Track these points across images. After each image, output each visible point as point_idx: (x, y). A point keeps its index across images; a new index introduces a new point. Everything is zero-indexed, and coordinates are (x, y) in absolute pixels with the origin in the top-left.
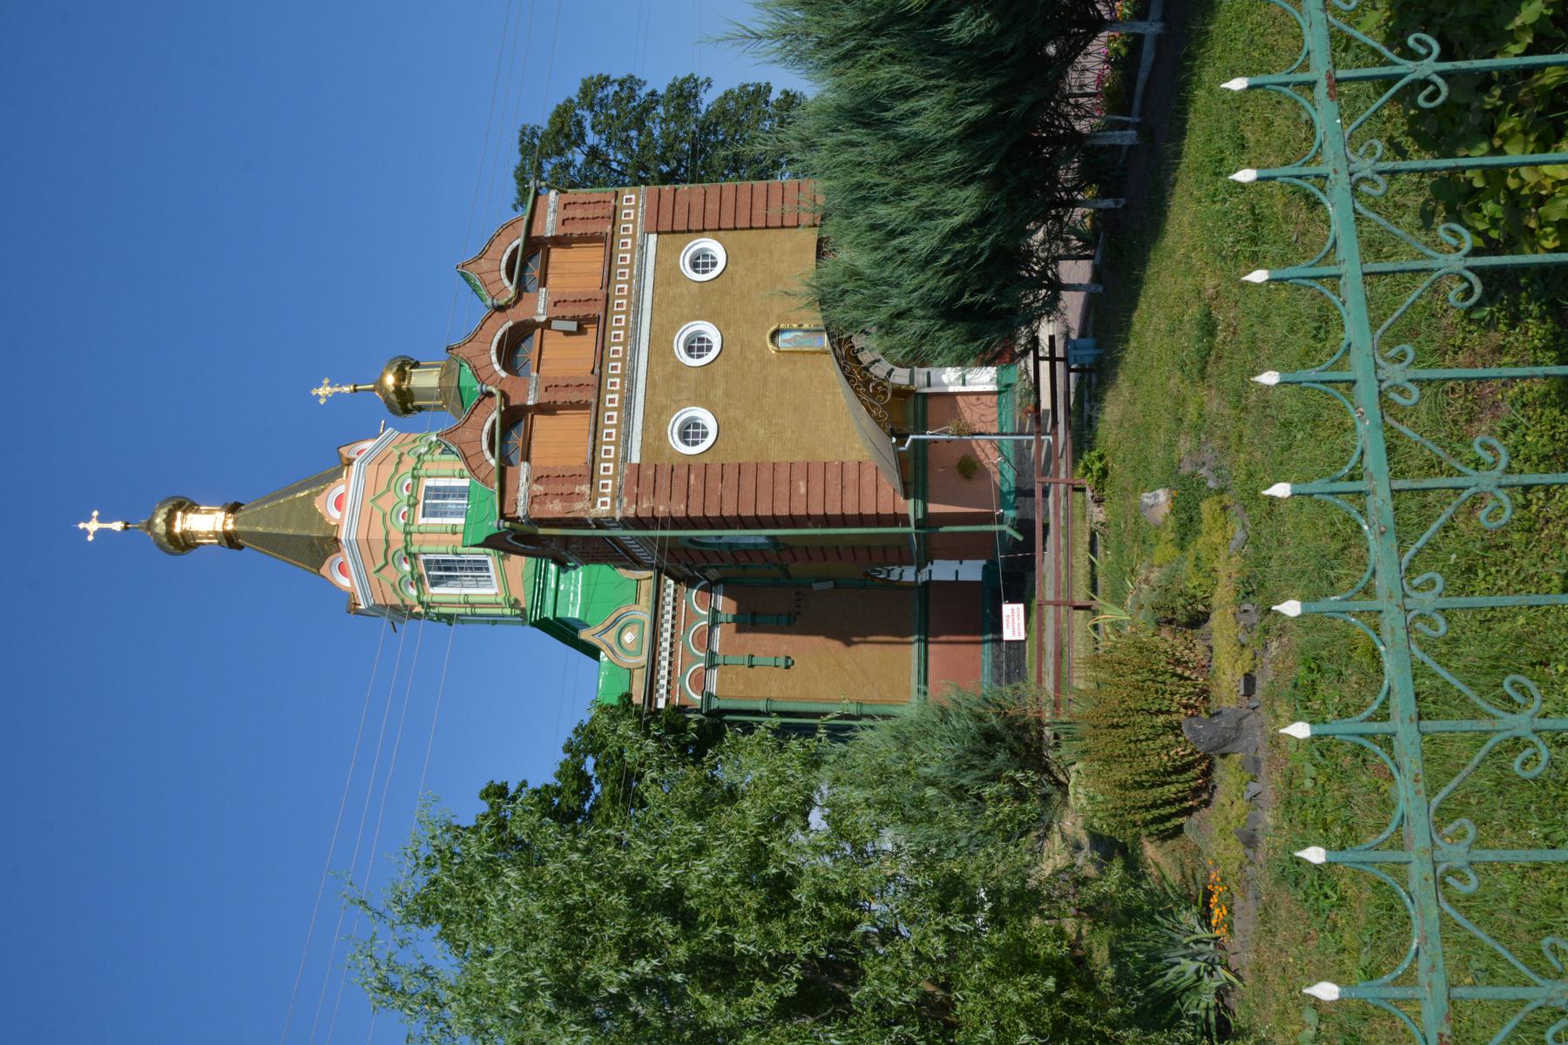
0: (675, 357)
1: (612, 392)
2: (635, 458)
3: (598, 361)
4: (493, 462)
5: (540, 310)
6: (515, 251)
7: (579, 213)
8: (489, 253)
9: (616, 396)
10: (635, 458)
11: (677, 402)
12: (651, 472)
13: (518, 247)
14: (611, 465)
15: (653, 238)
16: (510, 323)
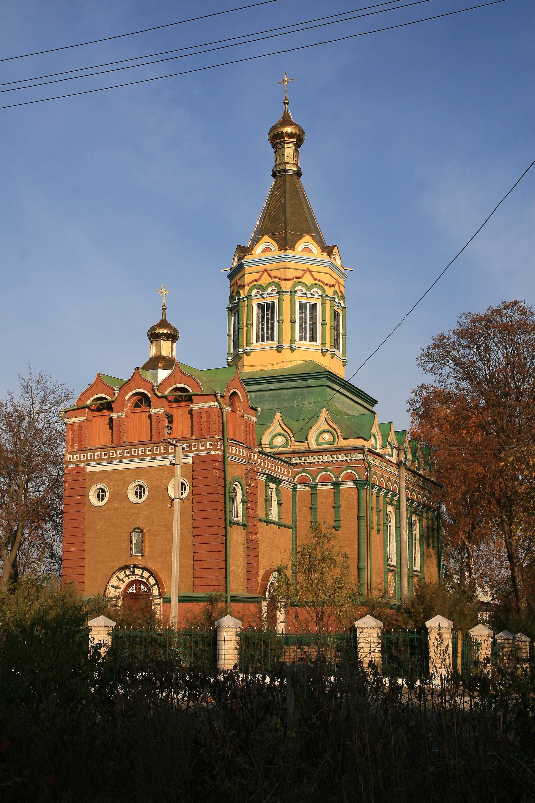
1: (116, 454)
2: (88, 469)
4: (89, 402)
5: (153, 411)
6: (185, 390)
7: (204, 419)
8: (184, 377)
10: (88, 469)
11: (113, 486)
12: (81, 478)
15: (190, 461)
16: (150, 395)
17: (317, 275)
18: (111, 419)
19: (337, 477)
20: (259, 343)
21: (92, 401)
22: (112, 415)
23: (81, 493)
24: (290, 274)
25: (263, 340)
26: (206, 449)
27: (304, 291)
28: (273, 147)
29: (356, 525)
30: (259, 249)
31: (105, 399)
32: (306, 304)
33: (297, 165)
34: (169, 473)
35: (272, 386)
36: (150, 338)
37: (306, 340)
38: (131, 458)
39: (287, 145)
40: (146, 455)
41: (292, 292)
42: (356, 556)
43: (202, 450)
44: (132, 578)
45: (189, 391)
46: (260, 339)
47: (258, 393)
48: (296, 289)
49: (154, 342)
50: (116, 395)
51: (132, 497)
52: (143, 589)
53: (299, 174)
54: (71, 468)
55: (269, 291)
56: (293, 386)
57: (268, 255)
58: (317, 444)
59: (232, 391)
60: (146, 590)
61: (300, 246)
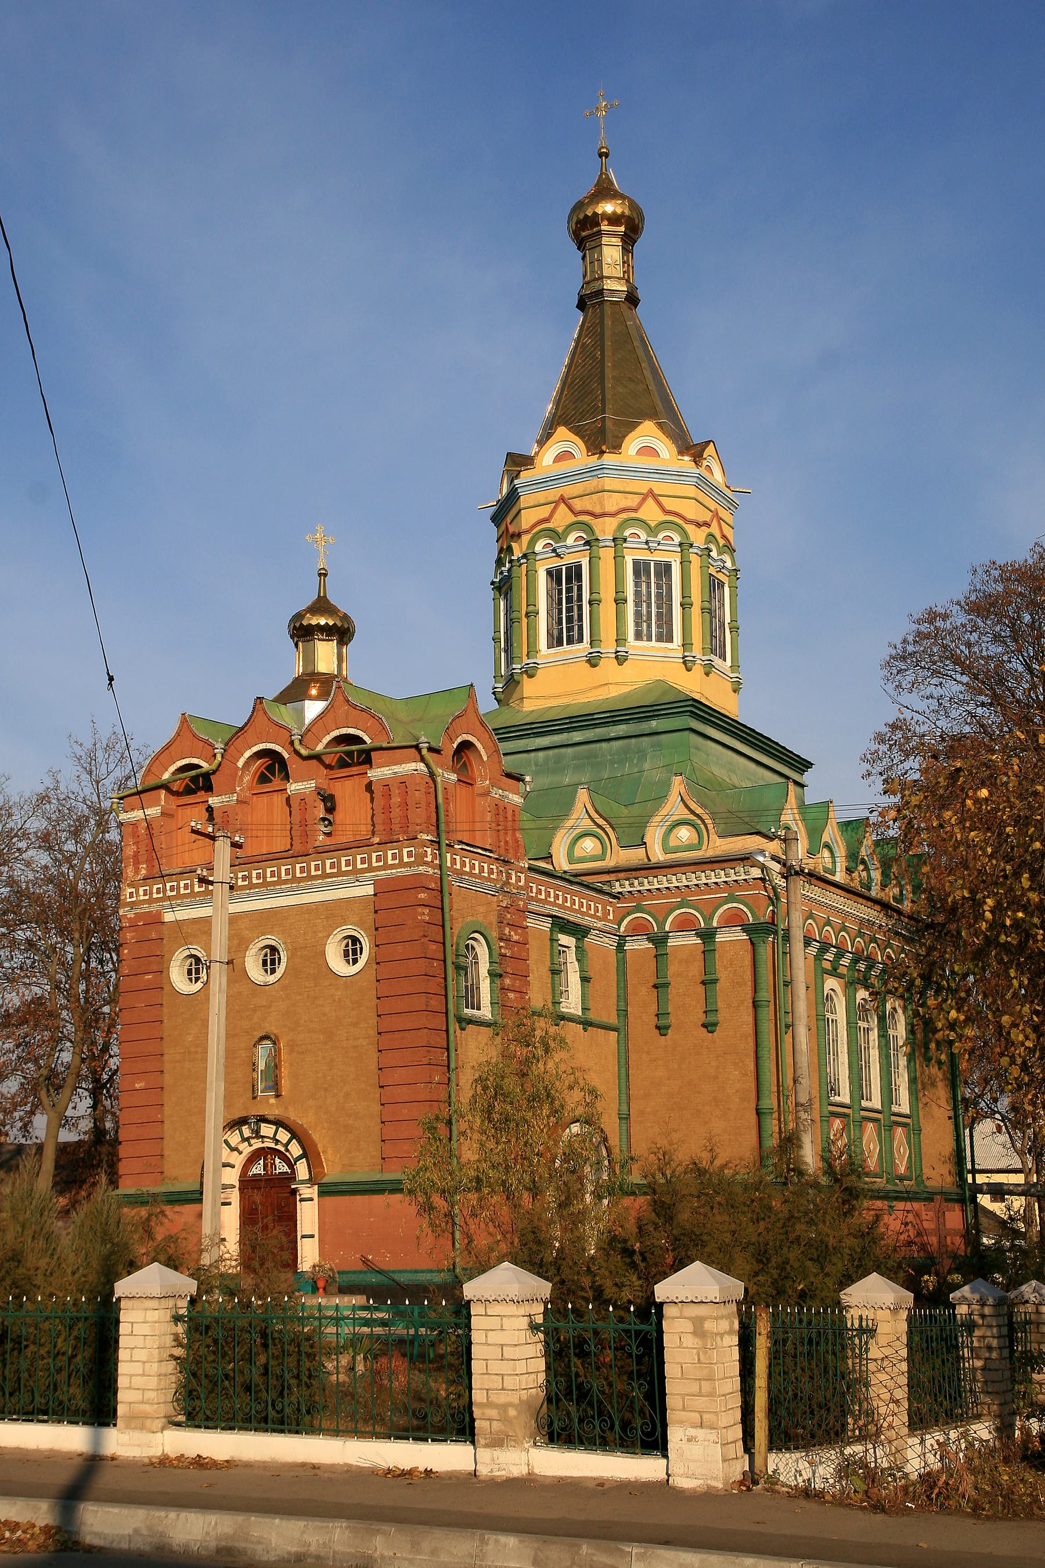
2: (168, 917)
3: (246, 860)
4: (166, 776)
7: (396, 800)
10: (168, 917)
12: (154, 936)
15: (370, 890)
16: (286, 755)
17: (669, 504)
18: (210, 810)
19: (709, 919)
20: (552, 651)
21: (173, 774)
22: (211, 801)
23: (155, 968)
24: (611, 503)
25: (560, 643)
26: (402, 864)
27: (644, 537)
28: (579, 249)
29: (750, 1019)
30: (547, 458)
31: (198, 767)
32: (647, 564)
33: (628, 281)
34: (327, 918)
35: (577, 736)
36: (292, 637)
37: (650, 639)
38: (250, 889)
39: (605, 240)
40: (280, 882)
41: (618, 541)
42: (753, 1085)
43: (392, 866)
44: (257, 1144)
45: (364, 742)
46: (555, 641)
47: (551, 752)
48: (627, 533)
49: (300, 644)
50: (219, 758)
51: (256, 972)
52: (281, 1167)
53: (632, 299)
54: (133, 916)
55: (570, 540)
56: (621, 734)
57: (566, 467)
58: (666, 850)
59: (459, 740)
60: (286, 1169)
61: (632, 444)
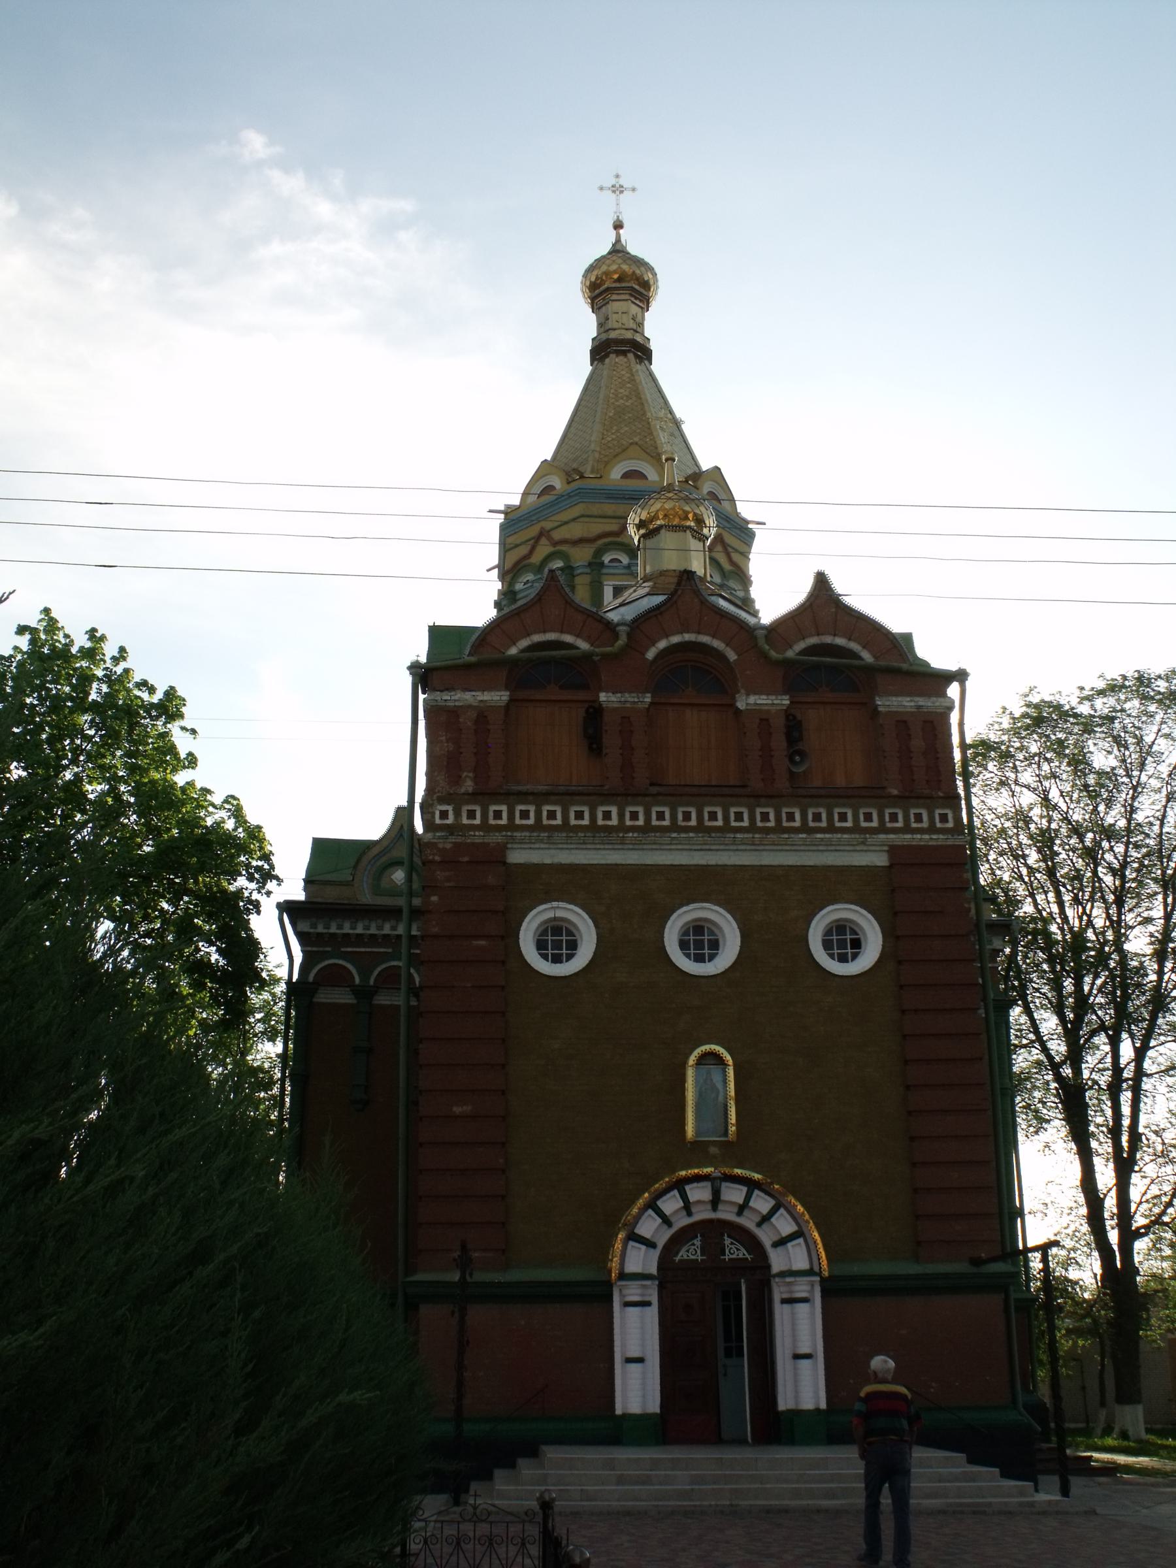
0: (682, 905)
1: (621, 816)
2: (517, 857)
4: (513, 651)
5: (752, 699)
7: (917, 743)
9: (614, 822)
13: (860, 658)
14: (504, 821)
18: (595, 713)
54: (448, 846)
60: (742, 1253)
